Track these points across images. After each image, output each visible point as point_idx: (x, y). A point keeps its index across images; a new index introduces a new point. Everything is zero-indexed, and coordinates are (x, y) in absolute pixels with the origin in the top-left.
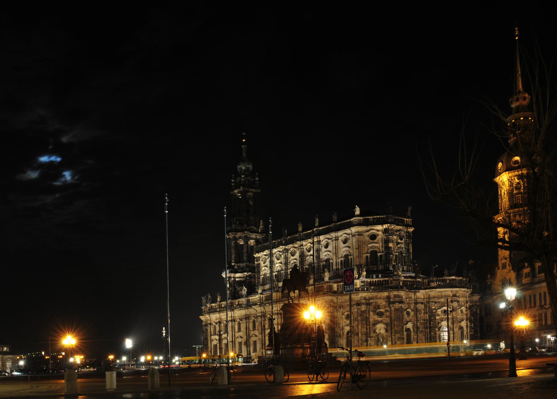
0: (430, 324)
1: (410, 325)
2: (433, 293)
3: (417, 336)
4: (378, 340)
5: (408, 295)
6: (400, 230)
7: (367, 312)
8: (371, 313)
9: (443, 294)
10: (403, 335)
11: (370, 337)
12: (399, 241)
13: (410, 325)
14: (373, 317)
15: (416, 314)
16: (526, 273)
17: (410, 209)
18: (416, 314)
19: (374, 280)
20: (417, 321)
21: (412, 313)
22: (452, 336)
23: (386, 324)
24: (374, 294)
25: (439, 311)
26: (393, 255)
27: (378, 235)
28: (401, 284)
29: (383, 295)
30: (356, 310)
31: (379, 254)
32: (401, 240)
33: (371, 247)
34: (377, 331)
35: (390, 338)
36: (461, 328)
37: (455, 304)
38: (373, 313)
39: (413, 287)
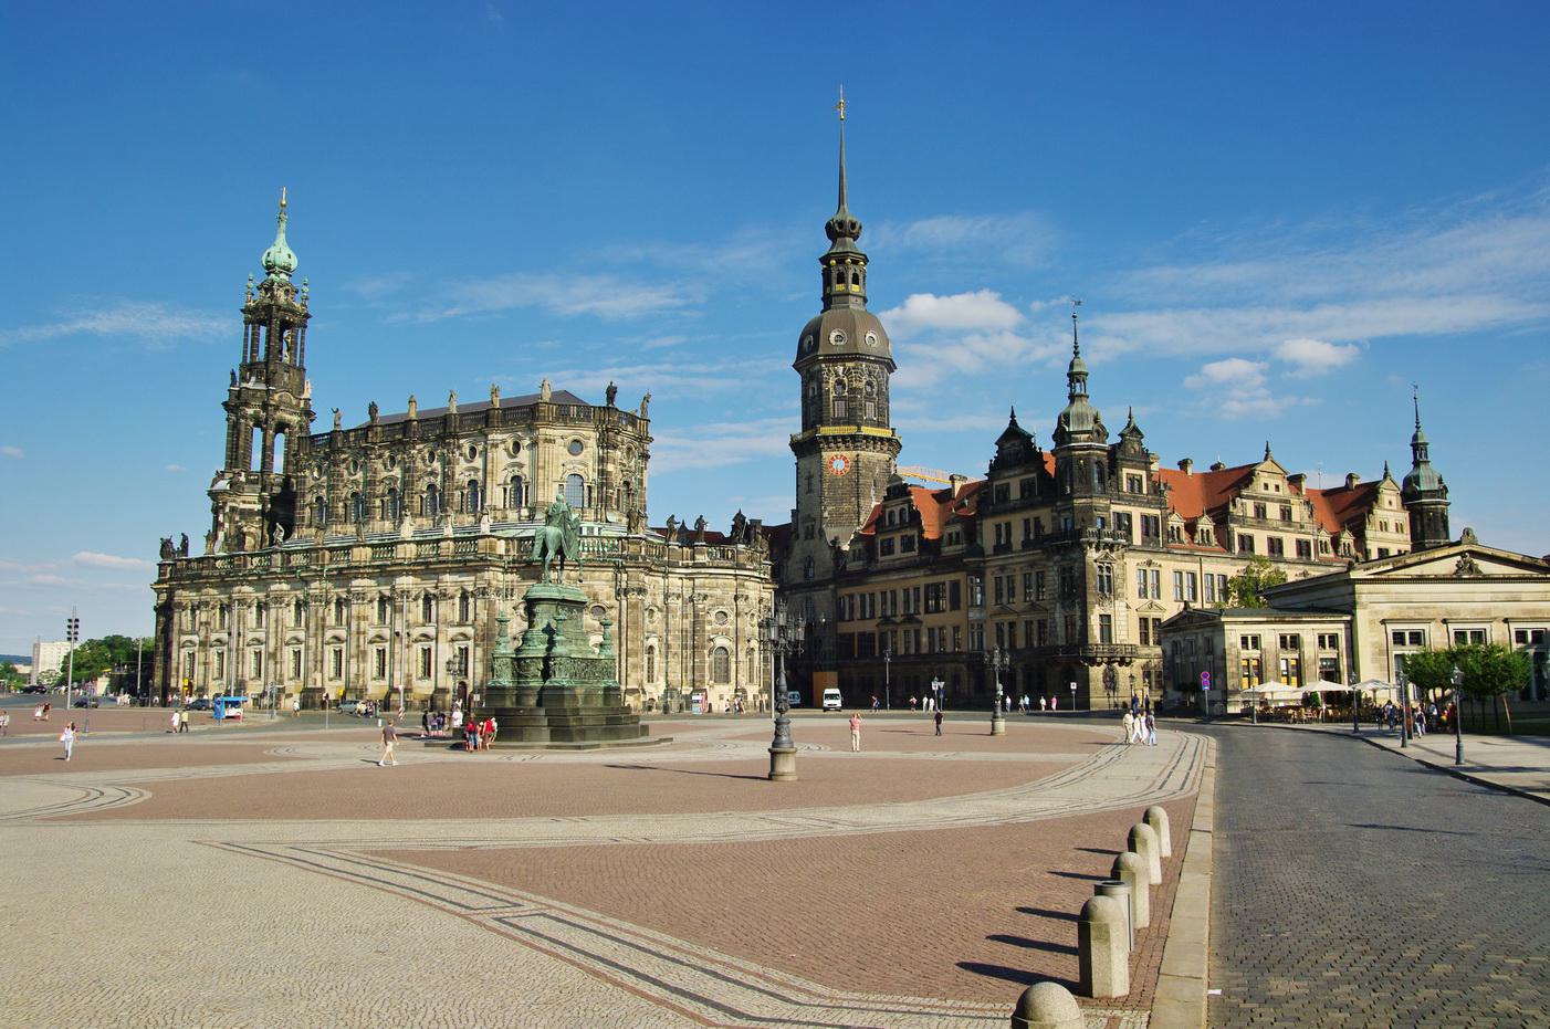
3: (667, 663)
13: (653, 641)
18: (667, 617)
20: (667, 631)
37: (741, 603)
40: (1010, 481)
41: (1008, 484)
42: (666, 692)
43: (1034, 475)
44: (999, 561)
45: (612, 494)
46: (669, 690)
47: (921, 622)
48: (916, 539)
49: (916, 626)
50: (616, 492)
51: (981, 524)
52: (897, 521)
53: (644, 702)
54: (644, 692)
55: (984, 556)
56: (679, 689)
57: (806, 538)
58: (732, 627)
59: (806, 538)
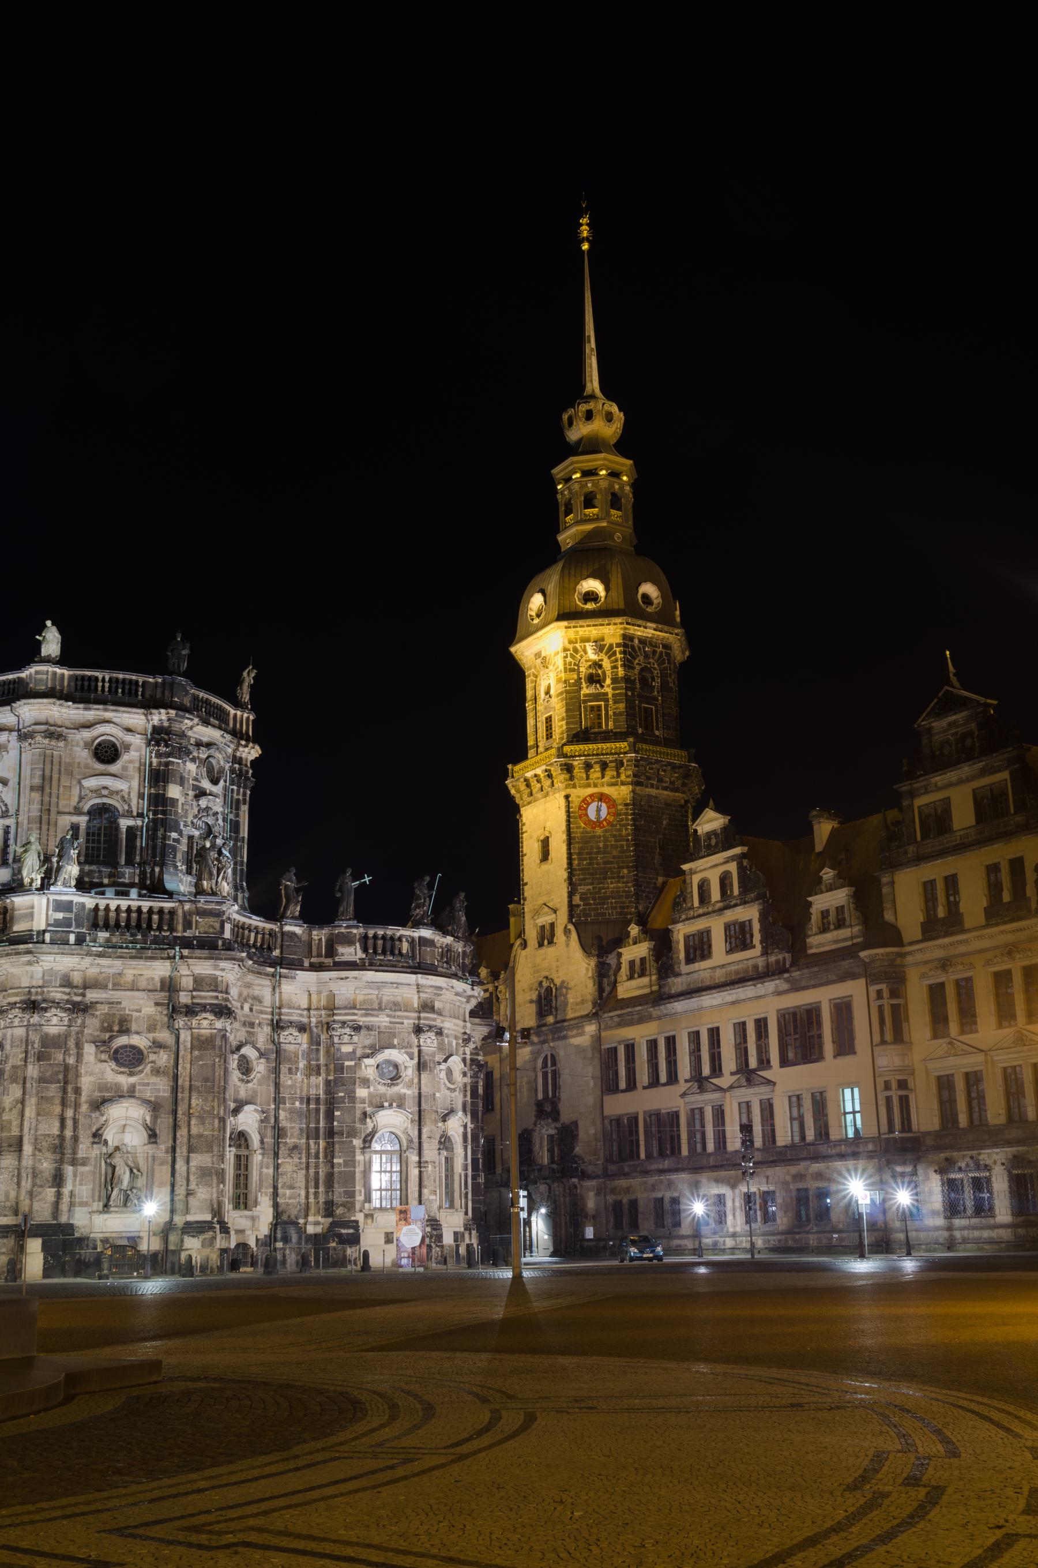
0: (330, 1116)
1: (248, 1120)
2: (352, 987)
3: (277, 1167)
4: (111, 1179)
5: (248, 985)
6: (209, 745)
7: (71, 1043)
8: (89, 1049)
9: (389, 995)
10: (222, 1158)
11: (74, 1163)
12: (206, 784)
13: (248, 1120)
14: (95, 1070)
15: (276, 1071)
16: (632, 963)
17: (249, 676)
18: (276, 1071)
19: (113, 904)
20: (278, 1100)
21: (260, 1068)
22: (414, 1172)
23: (155, 1107)
24: (110, 966)
25: (369, 1068)
26: (181, 834)
27: (127, 747)
28: (227, 935)
29: (148, 973)
30: (20, 1032)
31: (124, 823)
32: (215, 782)
33: (97, 792)
34: (110, 1135)
35: (163, 1172)
36: (445, 1142)
37: (429, 1042)
38: (99, 1051)
39: (273, 957)
40: (952, 793)
41: (947, 801)
42: (274, 1227)
43: (1005, 775)
44: (936, 949)
45: (177, 841)
46: (281, 1222)
47: (774, 1084)
48: (756, 926)
49: (763, 1092)
50: (185, 841)
51: (893, 883)
52: (715, 894)
53: (223, 1251)
54: (225, 1230)
55: (901, 944)
56: (301, 1221)
57: (541, 945)
58: (410, 1092)
59: (541, 945)
